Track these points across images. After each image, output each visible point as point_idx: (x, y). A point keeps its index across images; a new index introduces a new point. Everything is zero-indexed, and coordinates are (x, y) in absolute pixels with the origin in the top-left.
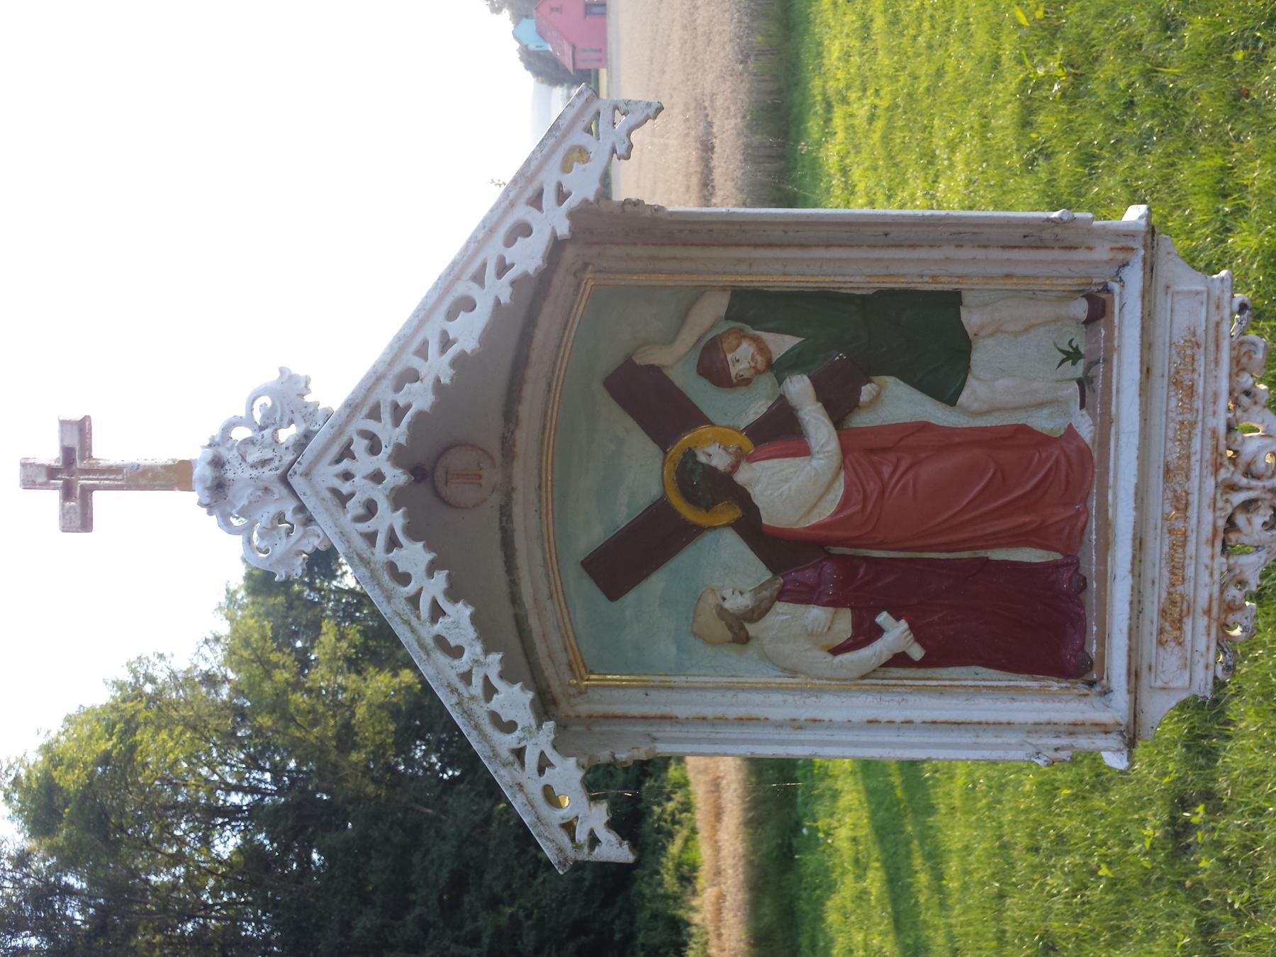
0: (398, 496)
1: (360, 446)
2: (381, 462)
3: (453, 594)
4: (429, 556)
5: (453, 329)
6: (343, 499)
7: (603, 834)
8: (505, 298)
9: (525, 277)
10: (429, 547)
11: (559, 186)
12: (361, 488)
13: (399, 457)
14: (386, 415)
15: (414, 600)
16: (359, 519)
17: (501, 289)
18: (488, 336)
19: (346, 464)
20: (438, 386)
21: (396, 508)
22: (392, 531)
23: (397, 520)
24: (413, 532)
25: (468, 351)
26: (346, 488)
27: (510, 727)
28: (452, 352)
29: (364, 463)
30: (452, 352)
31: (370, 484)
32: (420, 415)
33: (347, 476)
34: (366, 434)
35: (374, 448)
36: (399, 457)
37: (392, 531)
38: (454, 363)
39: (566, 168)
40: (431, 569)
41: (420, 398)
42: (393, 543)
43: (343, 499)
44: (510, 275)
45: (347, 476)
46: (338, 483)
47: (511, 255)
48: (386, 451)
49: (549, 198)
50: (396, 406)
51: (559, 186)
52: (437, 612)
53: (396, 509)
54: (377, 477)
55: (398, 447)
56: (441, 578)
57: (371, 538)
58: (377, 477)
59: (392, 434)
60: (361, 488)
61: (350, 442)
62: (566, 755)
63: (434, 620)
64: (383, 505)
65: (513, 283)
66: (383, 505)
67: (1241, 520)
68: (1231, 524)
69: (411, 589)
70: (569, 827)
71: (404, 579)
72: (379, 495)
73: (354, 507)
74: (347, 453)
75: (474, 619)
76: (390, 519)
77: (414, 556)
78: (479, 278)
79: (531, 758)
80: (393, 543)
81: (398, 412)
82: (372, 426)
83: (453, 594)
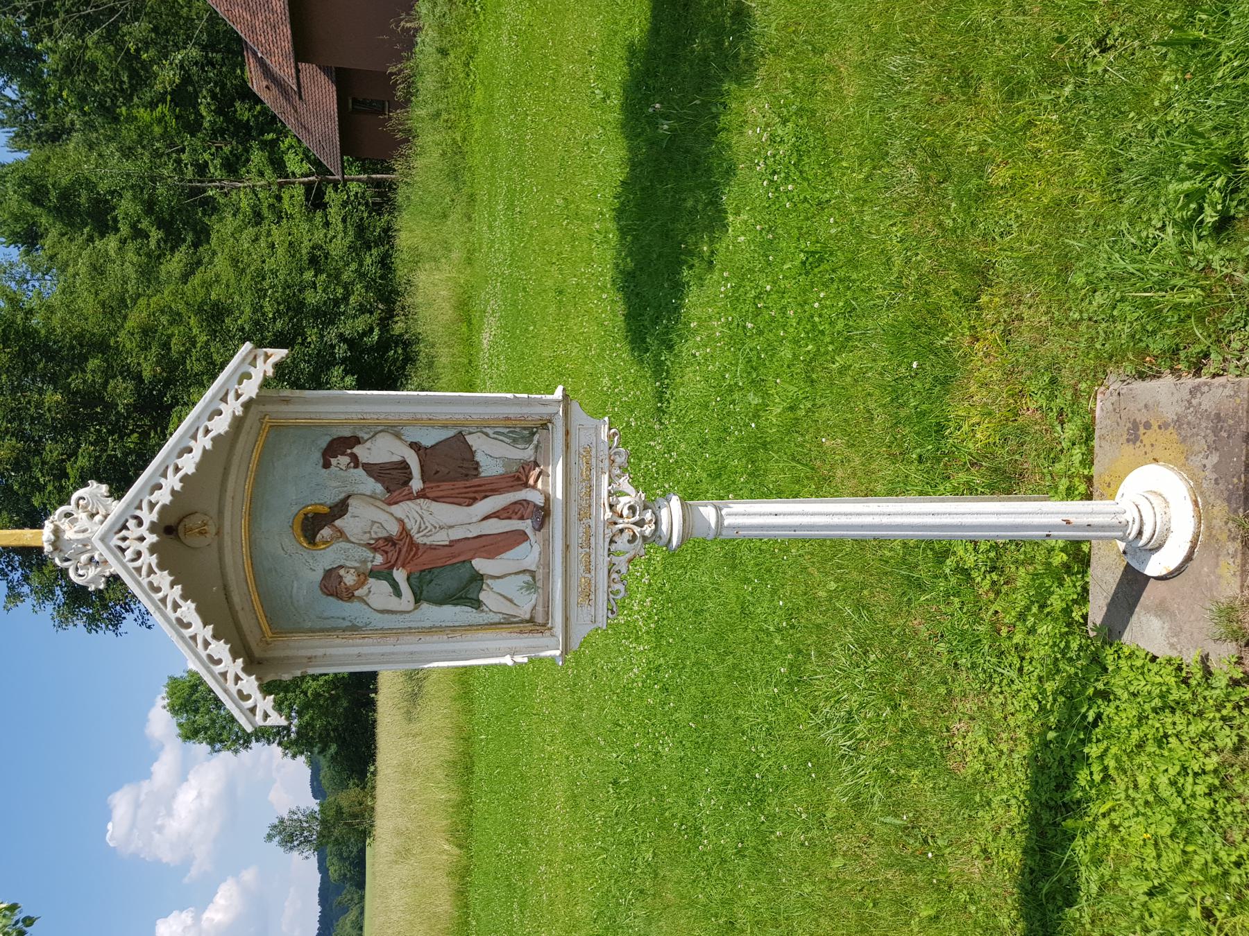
0: (153, 549)
1: (131, 523)
2: (143, 531)
3: (185, 597)
4: (172, 578)
5: (180, 462)
6: (123, 550)
7: (271, 712)
8: (209, 446)
9: (220, 435)
10: (170, 574)
11: (237, 391)
12: (133, 546)
13: (153, 528)
14: (145, 505)
15: (164, 600)
16: (133, 560)
17: (204, 442)
18: (199, 466)
19: (124, 533)
20: (173, 492)
21: (152, 554)
22: (150, 565)
23: (153, 560)
24: (162, 566)
25: (189, 473)
26: (124, 545)
27: (219, 662)
28: (180, 474)
29: (133, 531)
30: (180, 474)
31: (137, 543)
32: (164, 507)
33: (124, 539)
34: (136, 517)
35: (140, 524)
36: (153, 528)
37: (150, 566)
38: (181, 480)
39: (240, 383)
40: (172, 585)
41: (163, 497)
42: (151, 571)
43: (123, 550)
44: (211, 435)
45: (124, 539)
46: (120, 543)
47: (210, 425)
48: (146, 524)
49: (231, 396)
50: (150, 502)
51: (237, 391)
52: (176, 606)
53: (152, 554)
54: (142, 539)
55: (153, 523)
56: (178, 589)
57: (139, 570)
58: (142, 539)
59: (149, 517)
60: (133, 546)
61: (127, 521)
62: (250, 674)
63: (175, 611)
64: (145, 554)
65: (213, 439)
66: (145, 554)
67: (616, 539)
68: (612, 541)
69: (161, 595)
70: (253, 710)
71: (158, 590)
72: (143, 547)
73: (129, 554)
74: (124, 527)
75: (199, 610)
76: (149, 559)
77: (163, 579)
78: (194, 437)
79: (230, 677)
80: (151, 571)
81: (152, 506)
82: (138, 513)
83: (185, 597)
